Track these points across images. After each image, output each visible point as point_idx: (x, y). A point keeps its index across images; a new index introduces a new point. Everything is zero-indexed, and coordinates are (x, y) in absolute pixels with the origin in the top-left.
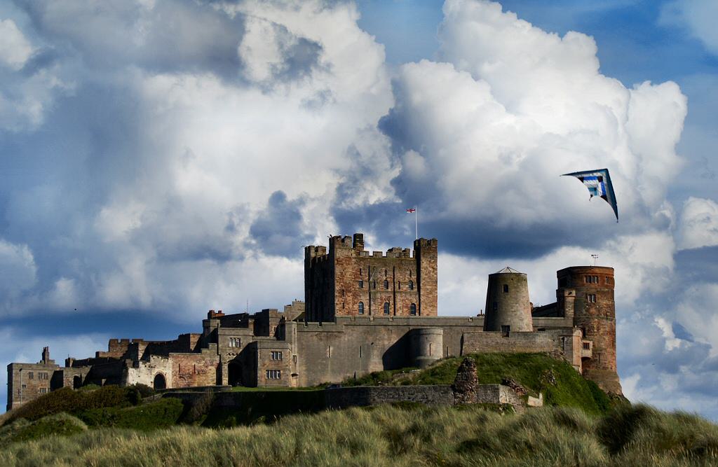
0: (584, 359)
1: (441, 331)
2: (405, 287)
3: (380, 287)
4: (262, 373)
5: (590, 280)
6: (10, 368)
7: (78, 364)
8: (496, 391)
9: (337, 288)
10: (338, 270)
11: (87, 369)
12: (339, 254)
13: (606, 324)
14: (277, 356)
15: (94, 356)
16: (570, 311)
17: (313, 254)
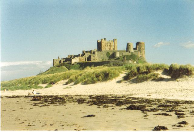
0: (140, 56)
1: (118, 52)
2: (112, 46)
3: (108, 46)
4: (92, 60)
5: (141, 44)
6: (53, 60)
7: (63, 59)
8: (129, 61)
9: (102, 46)
10: (102, 44)
11: (65, 60)
12: (102, 41)
13: (144, 51)
14: (94, 57)
15: (66, 57)
16: (138, 49)
17: (98, 42)
